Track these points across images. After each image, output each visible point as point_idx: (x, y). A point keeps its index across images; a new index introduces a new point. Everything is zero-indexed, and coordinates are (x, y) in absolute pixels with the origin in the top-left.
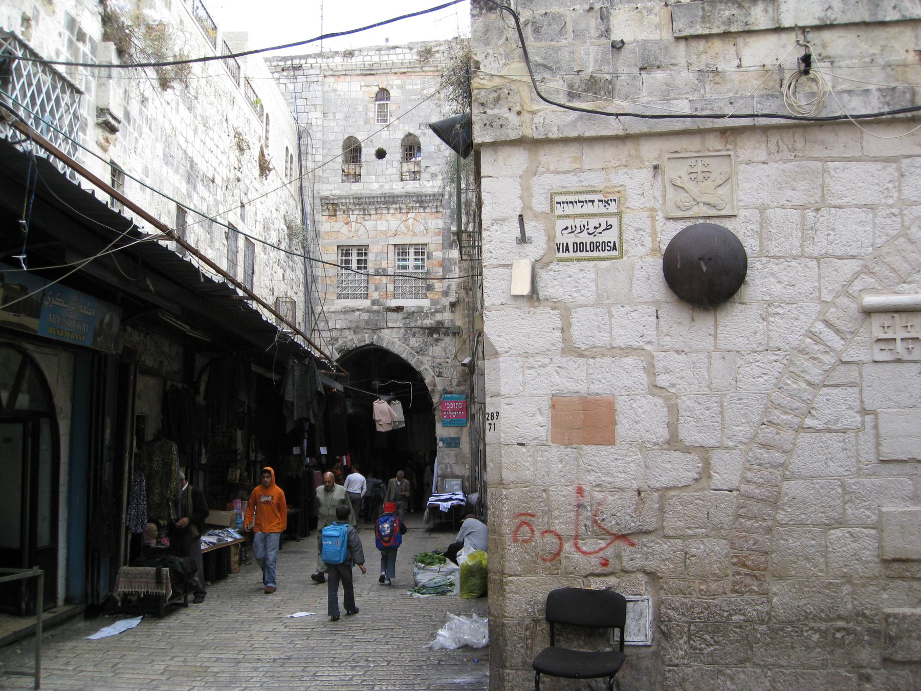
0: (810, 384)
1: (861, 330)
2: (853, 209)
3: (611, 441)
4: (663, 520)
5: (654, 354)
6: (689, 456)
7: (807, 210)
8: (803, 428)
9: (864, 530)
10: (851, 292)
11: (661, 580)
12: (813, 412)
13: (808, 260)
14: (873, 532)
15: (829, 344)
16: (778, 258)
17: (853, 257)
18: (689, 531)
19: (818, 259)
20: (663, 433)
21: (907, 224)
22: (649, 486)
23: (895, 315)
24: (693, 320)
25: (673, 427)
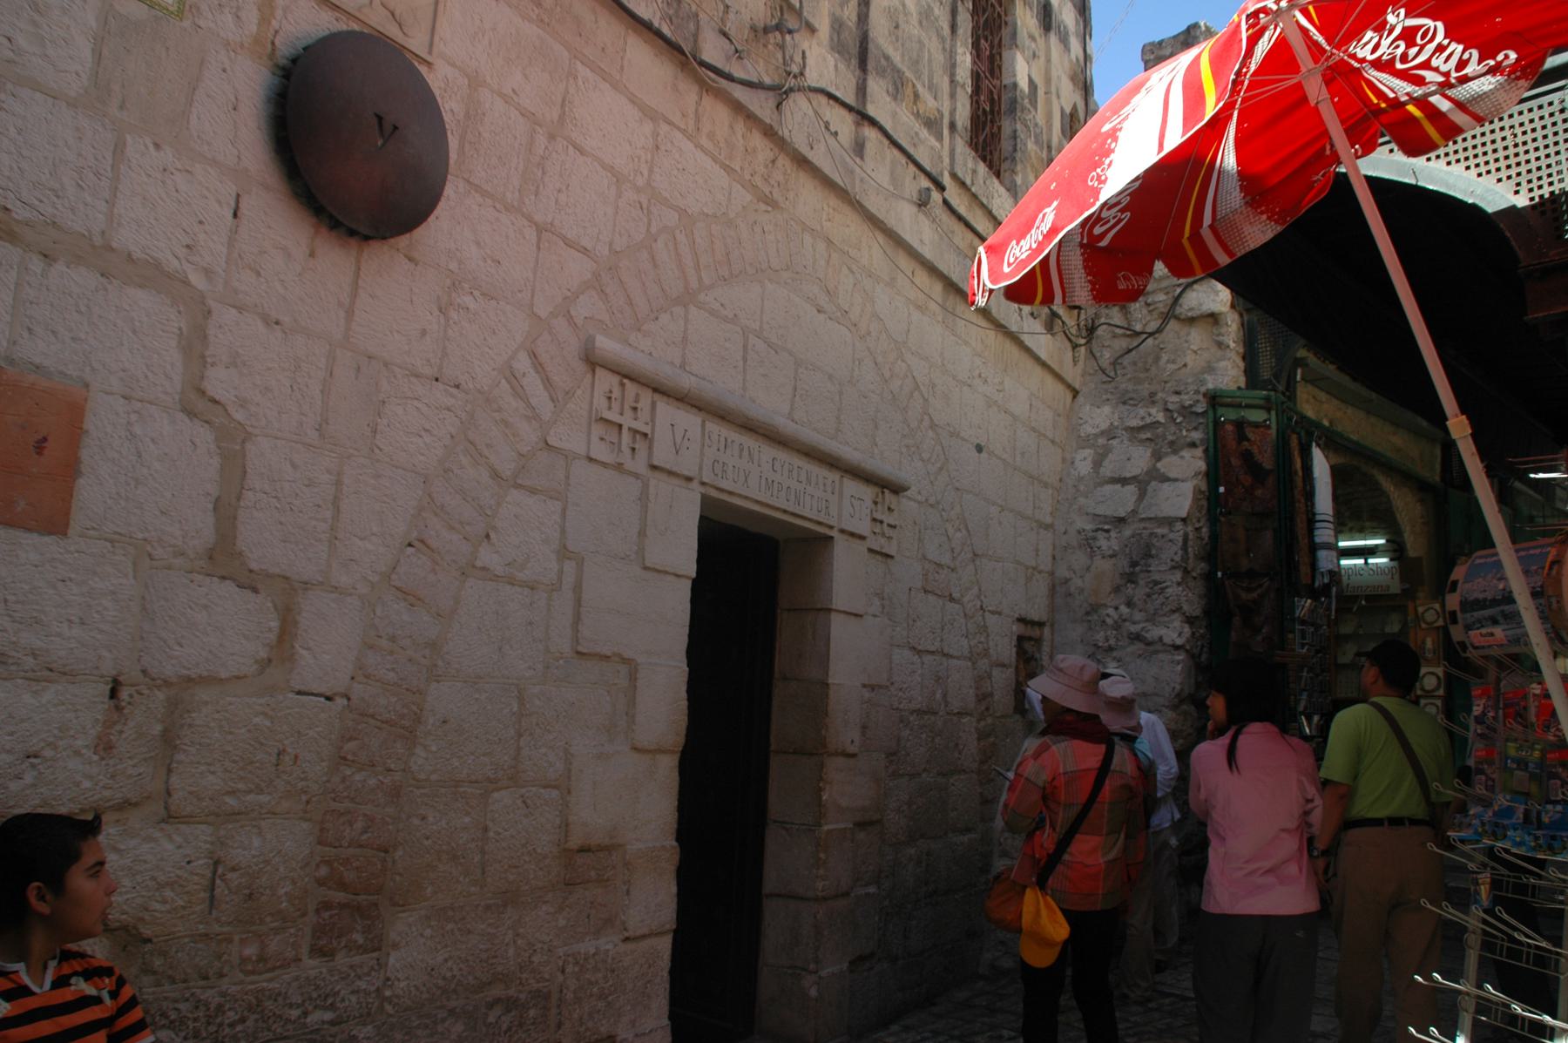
0: (496, 475)
1: (579, 392)
2: (596, 163)
3: (55, 524)
4: (169, 771)
5: (211, 303)
6: (251, 596)
7: (537, 128)
8: (474, 566)
9: (542, 791)
10: (573, 313)
11: (148, 947)
12: (492, 535)
13: (526, 223)
14: (555, 793)
15: (533, 401)
16: (485, 194)
17: (584, 251)
18: (231, 801)
19: (540, 229)
20: (201, 528)
21: (653, 230)
22: (144, 672)
23: (625, 381)
24: (312, 255)
25: (225, 512)
